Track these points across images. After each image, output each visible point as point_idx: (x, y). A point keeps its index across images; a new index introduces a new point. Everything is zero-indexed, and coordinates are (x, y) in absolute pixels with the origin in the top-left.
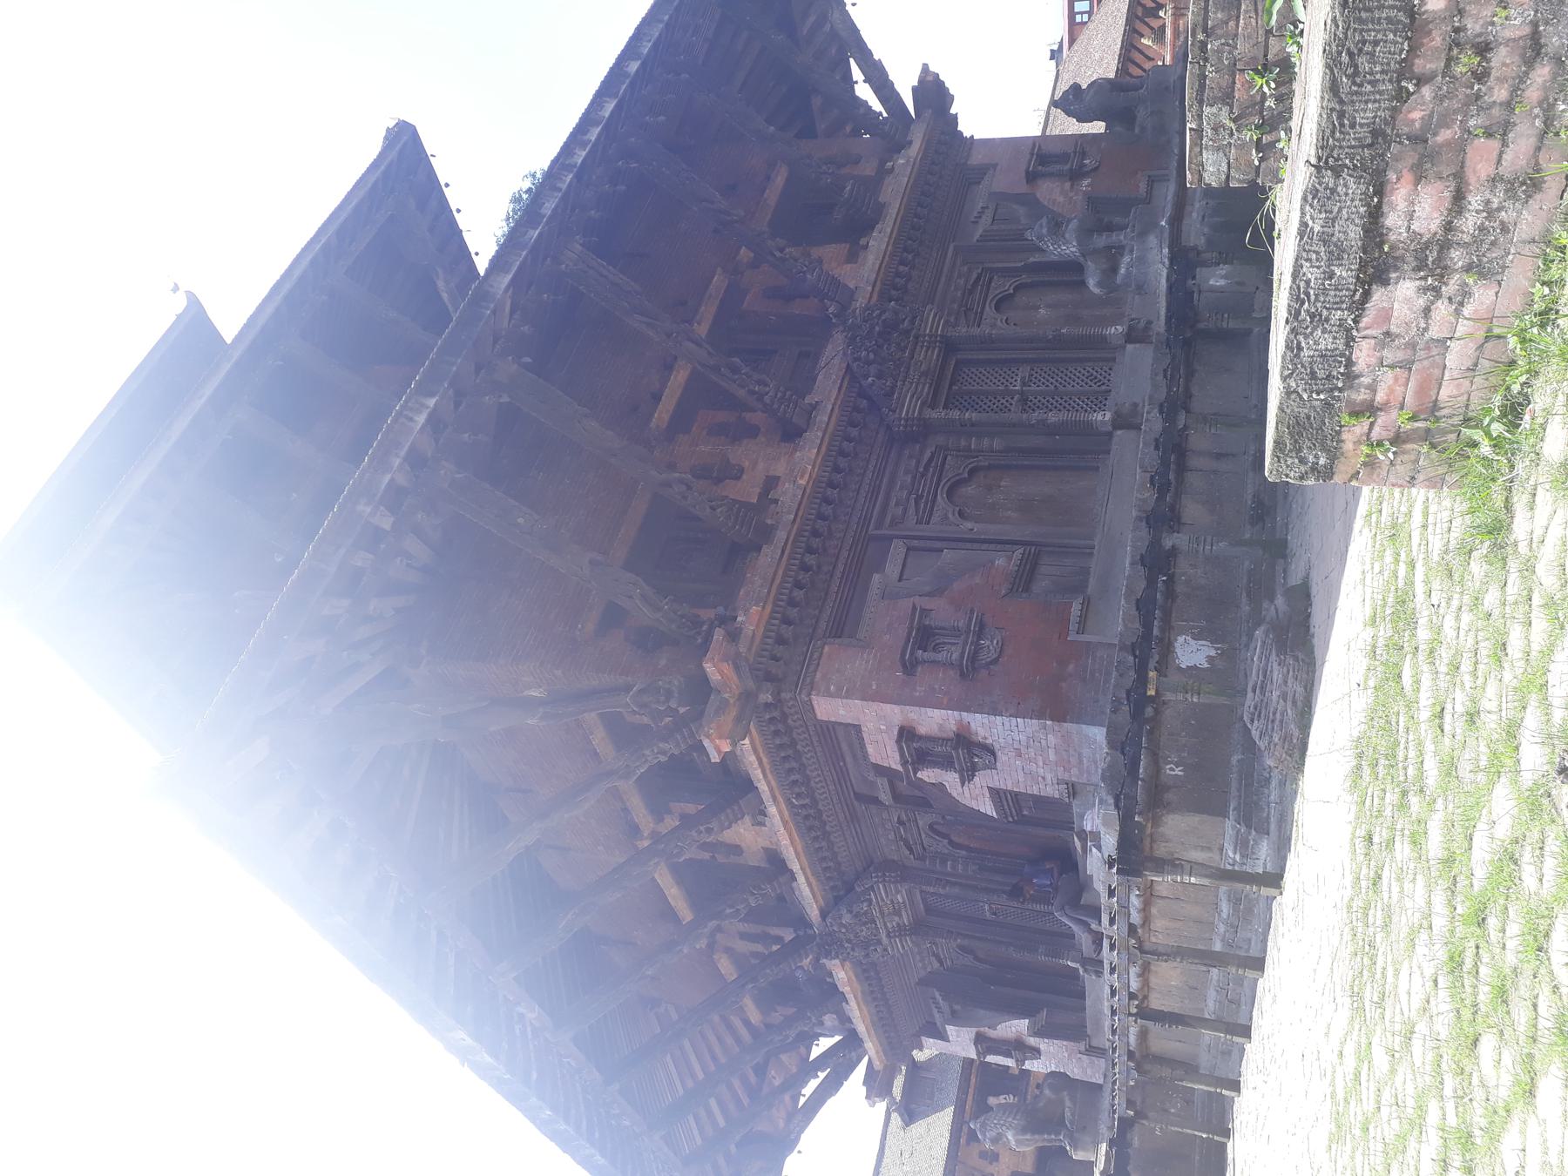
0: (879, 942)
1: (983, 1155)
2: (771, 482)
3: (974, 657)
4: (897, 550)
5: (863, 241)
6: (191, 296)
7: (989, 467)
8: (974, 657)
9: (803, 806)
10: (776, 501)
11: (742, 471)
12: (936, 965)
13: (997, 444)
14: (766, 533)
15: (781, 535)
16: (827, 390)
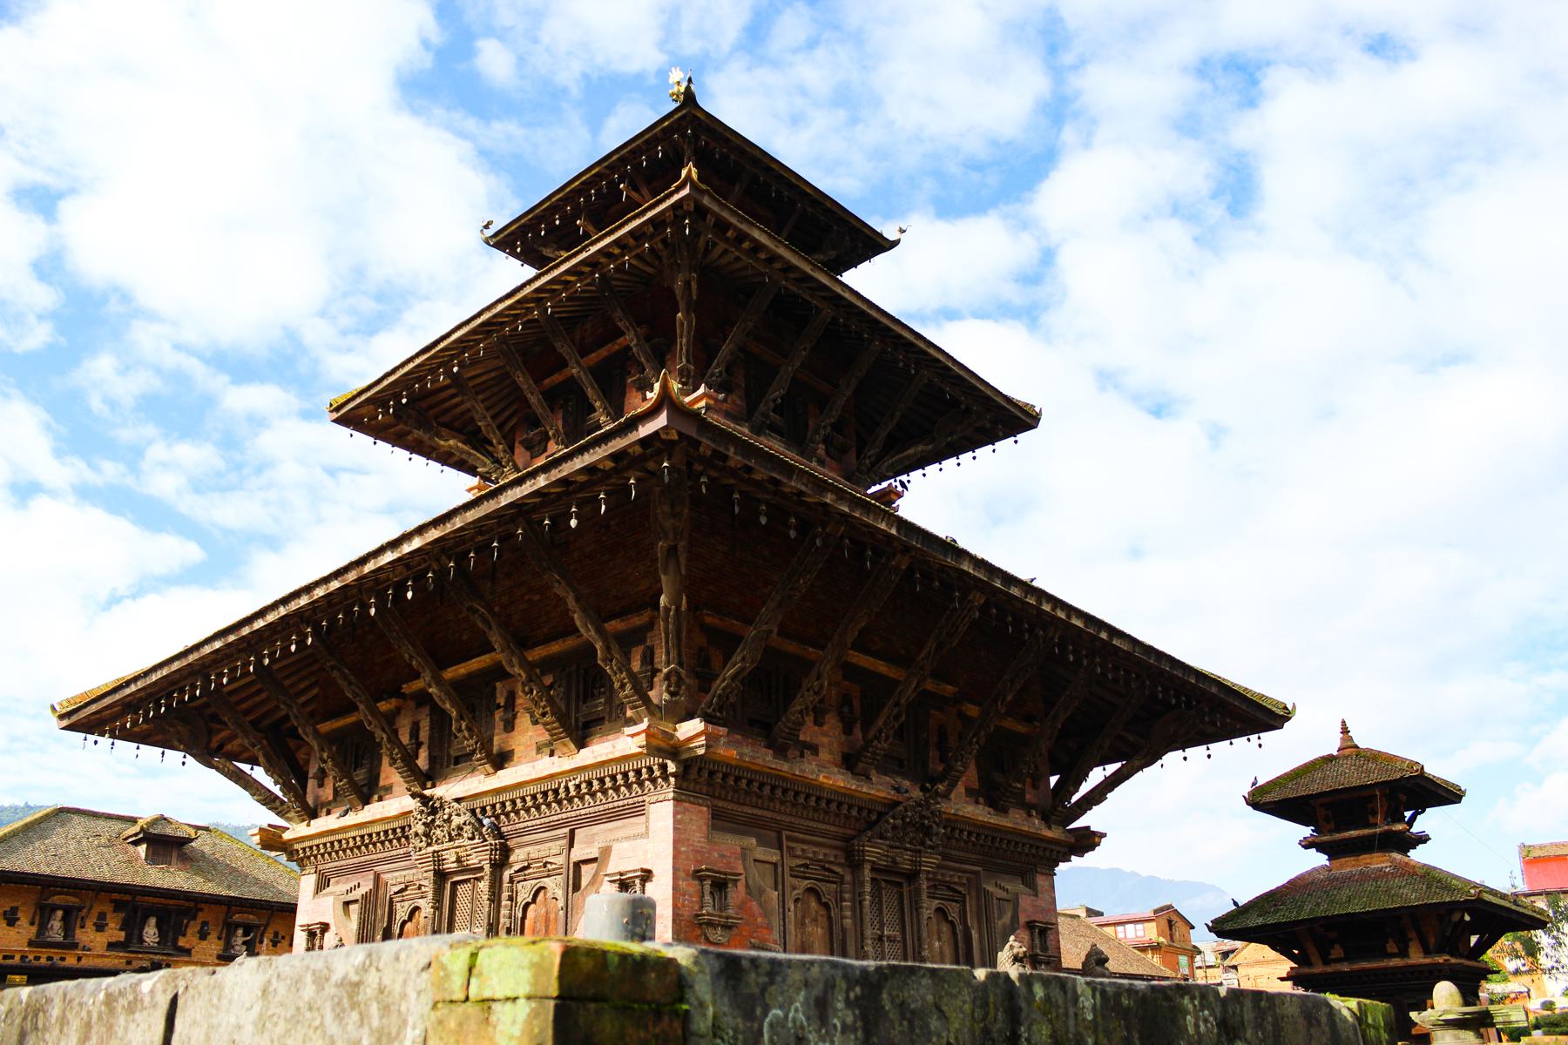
0: (429, 845)
1: (102, 916)
2: (814, 749)
3: (710, 924)
4: (774, 857)
5: (981, 800)
6: (895, 243)
7: (830, 918)
8: (710, 924)
9: (567, 789)
10: (802, 756)
11: (821, 725)
12: (396, 889)
13: (848, 922)
14: (781, 752)
15: (785, 767)
16: (878, 788)
